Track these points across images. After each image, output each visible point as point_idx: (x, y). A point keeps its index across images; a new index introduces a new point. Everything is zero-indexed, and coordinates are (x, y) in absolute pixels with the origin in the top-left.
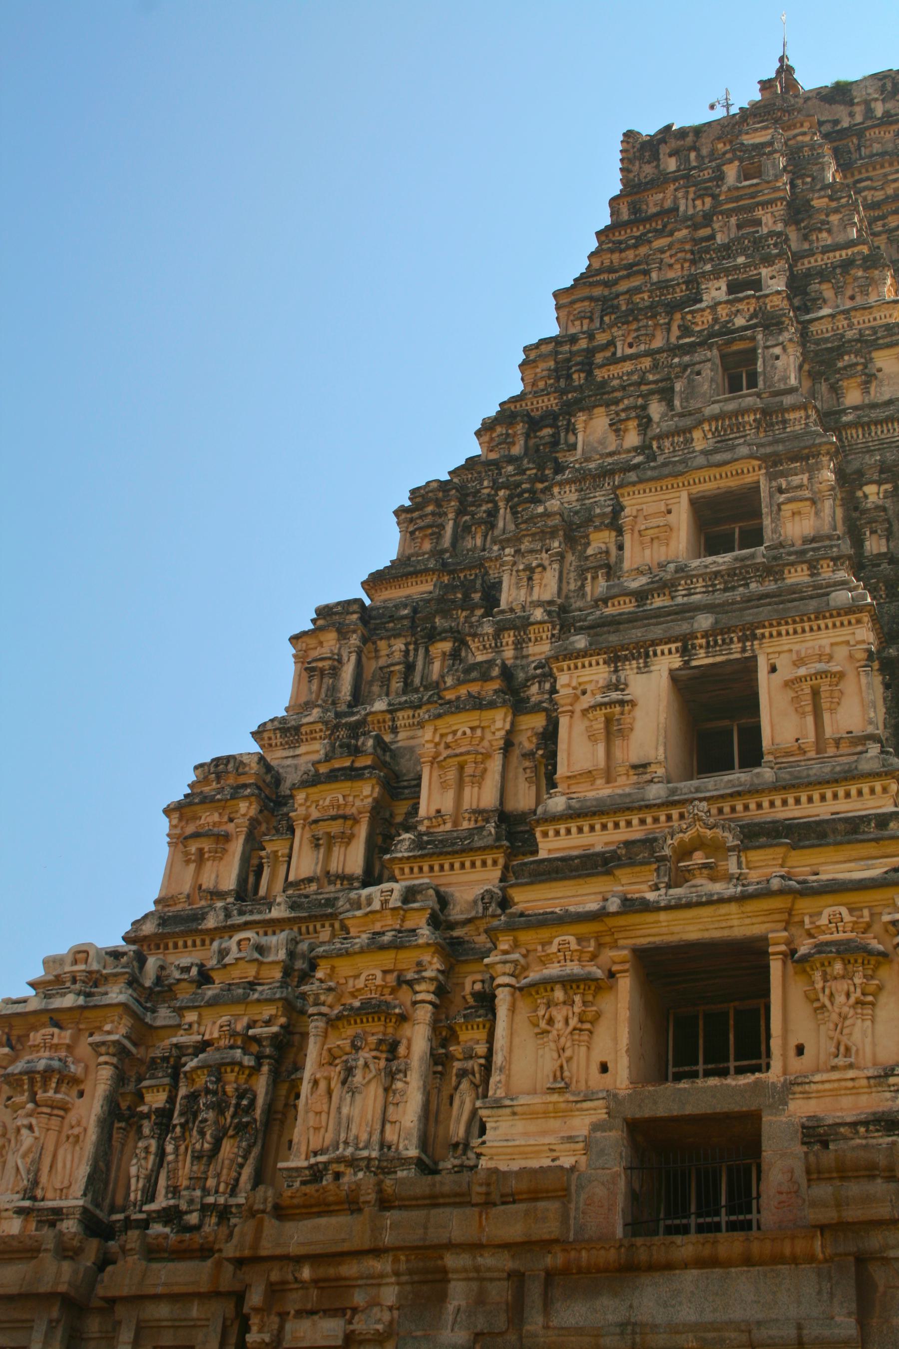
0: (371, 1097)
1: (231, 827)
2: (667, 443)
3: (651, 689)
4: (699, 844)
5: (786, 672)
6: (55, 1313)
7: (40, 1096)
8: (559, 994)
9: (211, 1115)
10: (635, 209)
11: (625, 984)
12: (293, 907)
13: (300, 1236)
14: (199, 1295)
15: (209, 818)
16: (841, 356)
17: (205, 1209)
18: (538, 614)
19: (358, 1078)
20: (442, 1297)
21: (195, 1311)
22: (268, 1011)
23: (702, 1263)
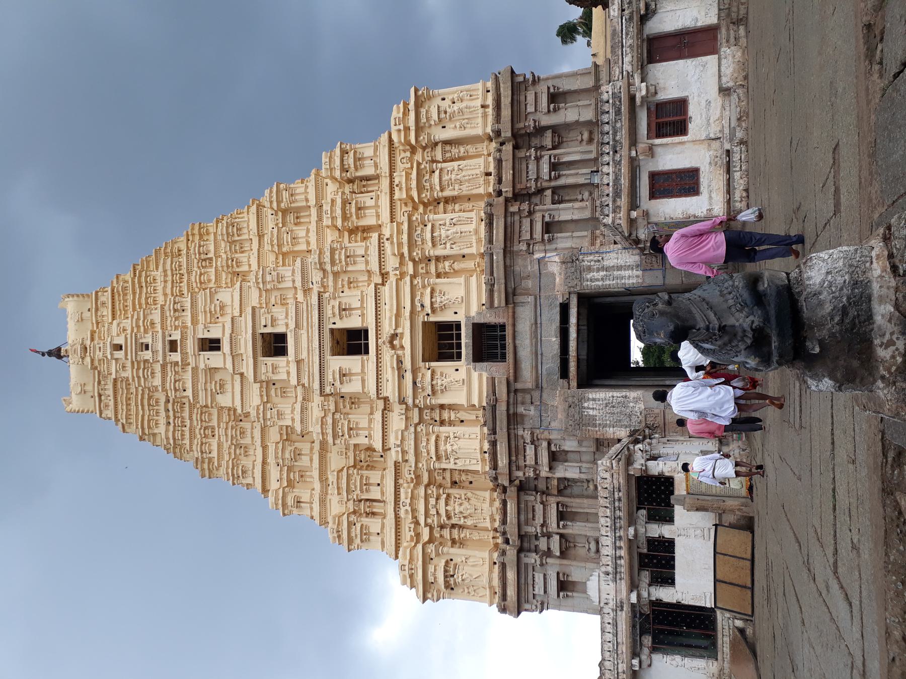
0: (461, 443)
1: (358, 526)
4: (391, 342)
5: (337, 320)
6: (522, 555)
8: (434, 382)
11: (433, 364)
13: (503, 461)
16: (210, 312)
19: (455, 447)
21: (522, 506)
22: (430, 492)
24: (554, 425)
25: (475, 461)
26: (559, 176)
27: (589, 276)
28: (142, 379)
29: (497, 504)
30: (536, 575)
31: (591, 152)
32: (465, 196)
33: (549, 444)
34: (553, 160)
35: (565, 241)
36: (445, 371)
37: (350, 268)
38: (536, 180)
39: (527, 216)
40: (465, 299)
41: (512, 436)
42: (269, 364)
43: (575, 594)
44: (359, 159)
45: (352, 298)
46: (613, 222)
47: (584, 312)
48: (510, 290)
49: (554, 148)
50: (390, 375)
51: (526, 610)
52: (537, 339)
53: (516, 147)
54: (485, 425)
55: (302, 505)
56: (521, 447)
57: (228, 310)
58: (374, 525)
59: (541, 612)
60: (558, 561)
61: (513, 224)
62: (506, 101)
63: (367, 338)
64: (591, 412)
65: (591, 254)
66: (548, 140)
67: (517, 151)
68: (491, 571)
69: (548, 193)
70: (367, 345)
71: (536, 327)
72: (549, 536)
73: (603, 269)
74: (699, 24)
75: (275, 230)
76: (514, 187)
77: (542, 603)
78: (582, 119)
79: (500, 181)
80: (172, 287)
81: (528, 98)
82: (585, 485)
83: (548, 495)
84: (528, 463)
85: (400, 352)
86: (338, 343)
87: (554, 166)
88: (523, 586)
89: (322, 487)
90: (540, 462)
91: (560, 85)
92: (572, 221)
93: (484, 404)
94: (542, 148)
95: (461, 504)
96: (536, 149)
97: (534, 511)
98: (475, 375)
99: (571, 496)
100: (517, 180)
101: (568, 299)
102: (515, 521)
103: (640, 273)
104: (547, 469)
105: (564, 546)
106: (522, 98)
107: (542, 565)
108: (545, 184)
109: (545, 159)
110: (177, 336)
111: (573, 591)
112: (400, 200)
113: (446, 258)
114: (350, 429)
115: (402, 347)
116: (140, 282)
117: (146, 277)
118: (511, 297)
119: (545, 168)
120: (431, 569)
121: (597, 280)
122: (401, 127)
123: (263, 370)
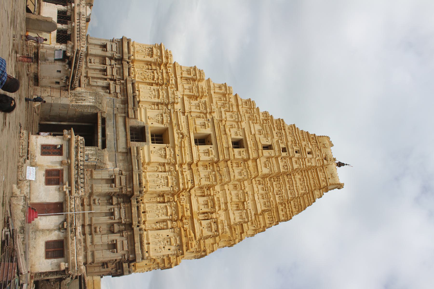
1: (192, 75)
3: (208, 131)
5: (210, 149)
16: (270, 163)
20: (122, 104)
24: (108, 100)
26: (110, 210)
28: (296, 139)
30: (115, 50)
33: (110, 93)
34: (113, 217)
35: (105, 175)
38: (120, 208)
40: (150, 152)
41: (126, 96)
44: (209, 227)
45: (204, 158)
48: (129, 154)
50: (183, 124)
52: (116, 134)
53: (131, 224)
57: (263, 165)
58: (185, 75)
61: (130, 184)
62: (137, 245)
64: (91, 97)
67: (131, 222)
68: (134, 52)
69: (114, 203)
71: (116, 138)
75: (247, 199)
76: (131, 204)
79: (138, 207)
80: (293, 184)
81: (127, 247)
84: (119, 86)
85: (179, 131)
86: (209, 142)
89: (210, 92)
91: (112, 254)
94: (119, 223)
95: (148, 76)
97: (117, 73)
98: (144, 120)
100: (130, 208)
102: (124, 68)
106: (130, 247)
107: (113, 54)
110: (284, 154)
114: (199, 106)
115: (178, 133)
116: (308, 187)
117: (306, 190)
118: (128, 152)
119: (116, 213)
120: (159, 54)
121: (89, 150)
122: (189, 237)
123: (241, 134)
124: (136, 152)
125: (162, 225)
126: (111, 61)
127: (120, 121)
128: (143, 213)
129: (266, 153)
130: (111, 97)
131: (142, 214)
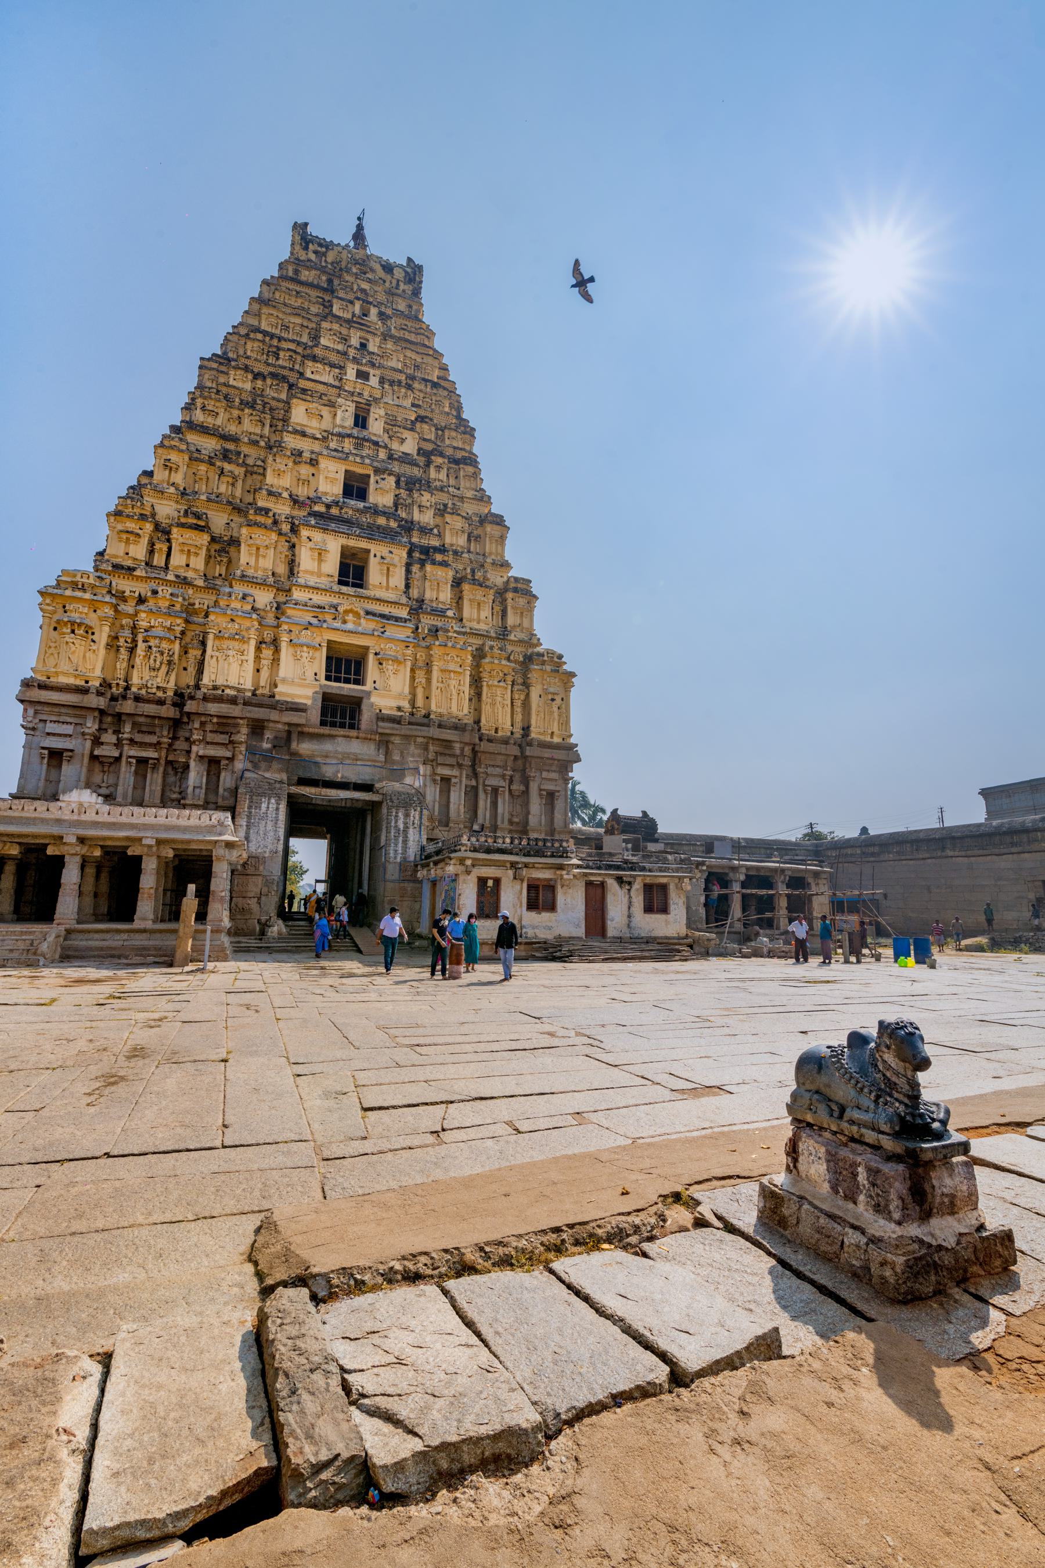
0: (235, 667)
2: (335, 438)
4: (351, 611)
6: (96, 714)
7: (76, 631)
8: (305, 648)
9: (158, 655)
10: (296, 272)
11: (325, 650)
12: (177, 576)
13: (213, 708)
14: (160, 718)
15: (131, 525)
17: (158, 687)
18: (285, 495)
23: (344, 736)
25: (213, 678)
26: (486, 794)
27: (400, 814)
29: (160, 694)
31: (503, 822)
32: (480, 706)
33: (228, 759)
35: (432, 794)
36: (317, 662)
37: (427, 584)
38: (486, 773)
39: (458, 763)
41: (241, 722)
42: (338, 476)
43: (45, 767)
46: (462, 844)
47: (360, 805)
48: (392, 739)
49: (510, 790)
51: (25, 710)
53: (516, 758)
54: (254, 694)
55: (167, 472)
56: (227, 729)
59: (23, 726)
60: (87, 752)
63: (354, 585)
64: (264, 806)
65: (421, 818)
66: (517, 787)
69: (474, 783)
70: (346, 584)
72: (118, 744)
73: (406, 828)
74: (609, 923)
77: (34, 729)
78: (530, 817)
79: (490, 741)
82: (177, 789)
83: (168, 750)
86: (354, 554)
87: (495, 790)
88: (57, 710)
90: (209, 747)
92: (448, 802)
93: (277, 698)
94: (511, 782)
96: (511, 777)
97: (150, 733)
98: (309, 692)
99: (165, 774)
100: (488, 755)
101: (378, 792)
102: (139, 711)
103: (398, 860)
104: (201, 753)
105: (104, 760)
106: (554, 768)
107: (83, 734)
108: (481, 781)
109: (502, 783)
110: (374, 381)
111: (49, 765)
112: (483, 645)
113: (429, 681)
122: (546, 658)
124: (391, 725)
125: (518, 703)
126: (102, 744)
127: (305, 748)
128: (496, 732)
129: (376, 427)
130: (241, 757)
131: (500, 734)
